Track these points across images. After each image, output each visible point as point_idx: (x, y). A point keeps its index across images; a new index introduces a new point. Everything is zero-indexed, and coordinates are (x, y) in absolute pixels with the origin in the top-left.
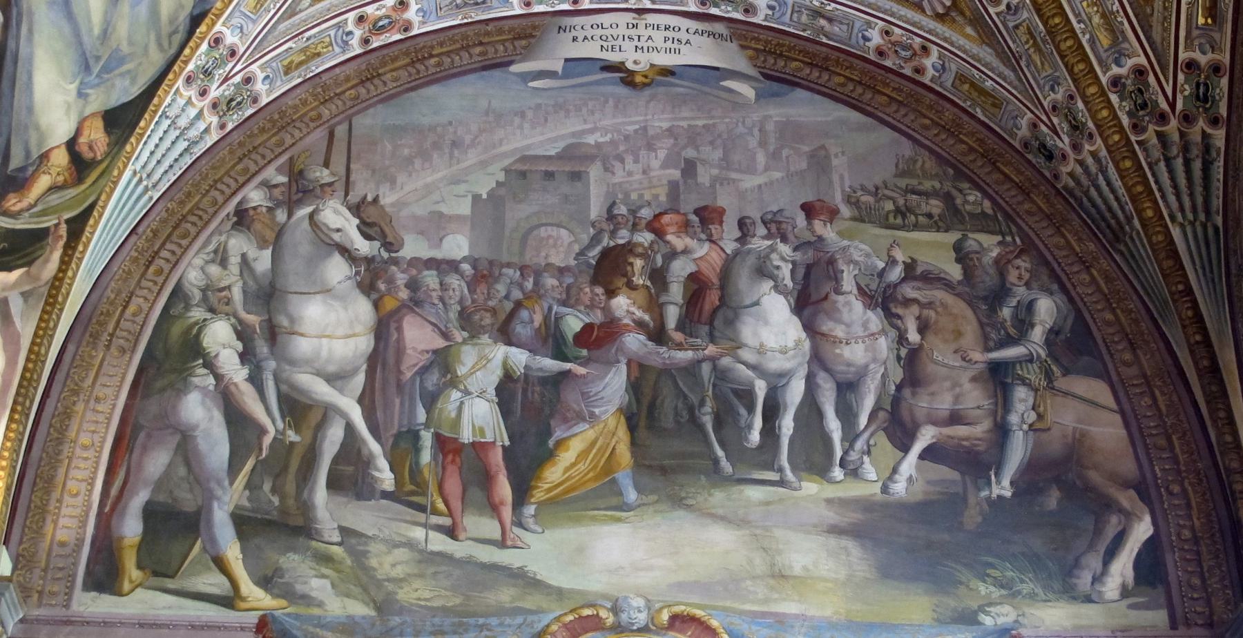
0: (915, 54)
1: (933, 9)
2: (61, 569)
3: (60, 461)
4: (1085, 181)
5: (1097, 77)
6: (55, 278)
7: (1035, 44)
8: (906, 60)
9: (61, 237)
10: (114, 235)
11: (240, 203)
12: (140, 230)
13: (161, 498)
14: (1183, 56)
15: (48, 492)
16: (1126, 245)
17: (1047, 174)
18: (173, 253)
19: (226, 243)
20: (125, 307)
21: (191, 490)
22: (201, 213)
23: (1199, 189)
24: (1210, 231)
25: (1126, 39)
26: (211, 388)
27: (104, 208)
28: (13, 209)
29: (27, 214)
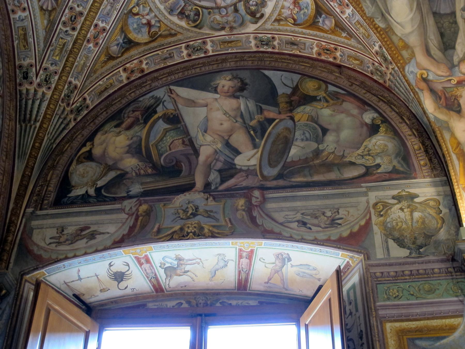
0: (19, 7)
1: (43, 4)
4: (31, 96)
5: (68, 76)
7: (62, 49)
8: (14, 5)
14: (86, 95)
16: (26, 126)
17: (18, 81)
23: (58, 133)
24: (51, 146)
25: (82, 75)
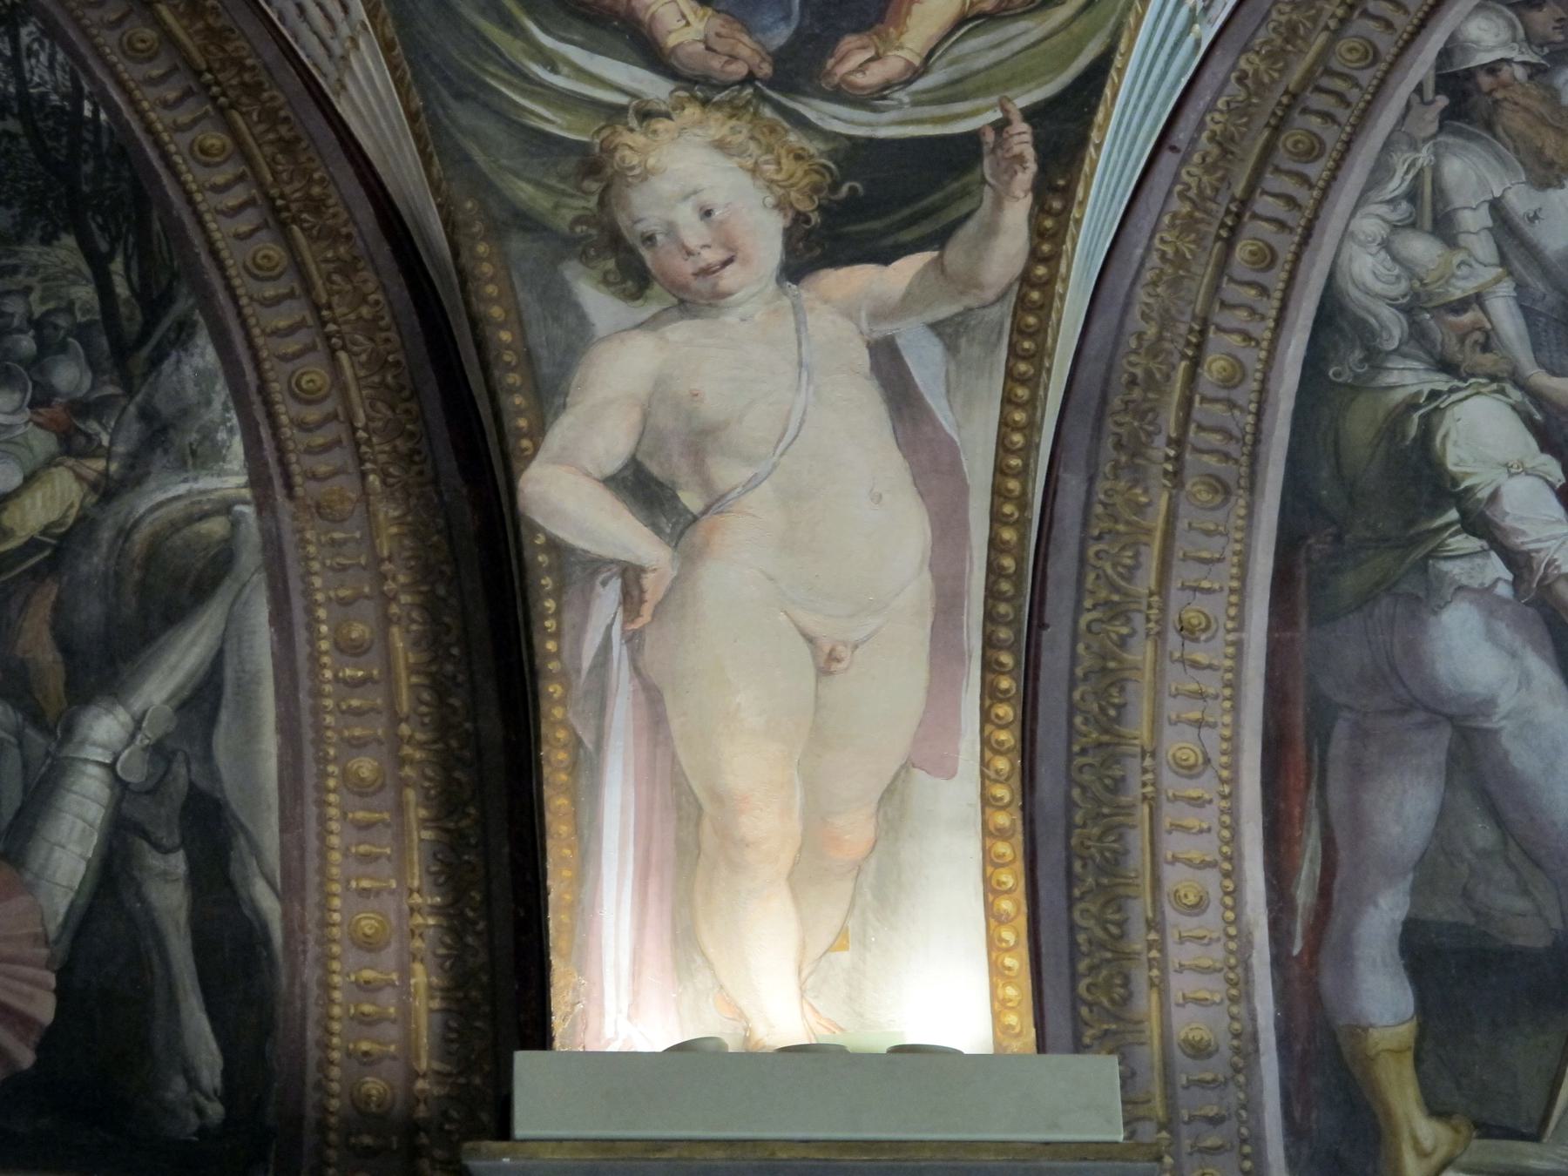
2: (1215, 1121)
3: (1128, 810)
6: (1026, 279)
9: (1020, 159)
10: (1129, 153)
11: (1445, 55)
12: (1181, 136)
13: (1444, 910)
15: (1114, 898)
18: (1291, 201)
19: (1436, 169)
20: (1196, 363)
21: (1526, 892)
22: (1339, 85)
26: (1504, 590)
27: (1121, 72)
28: (860, 79)
29: (903, 96)
